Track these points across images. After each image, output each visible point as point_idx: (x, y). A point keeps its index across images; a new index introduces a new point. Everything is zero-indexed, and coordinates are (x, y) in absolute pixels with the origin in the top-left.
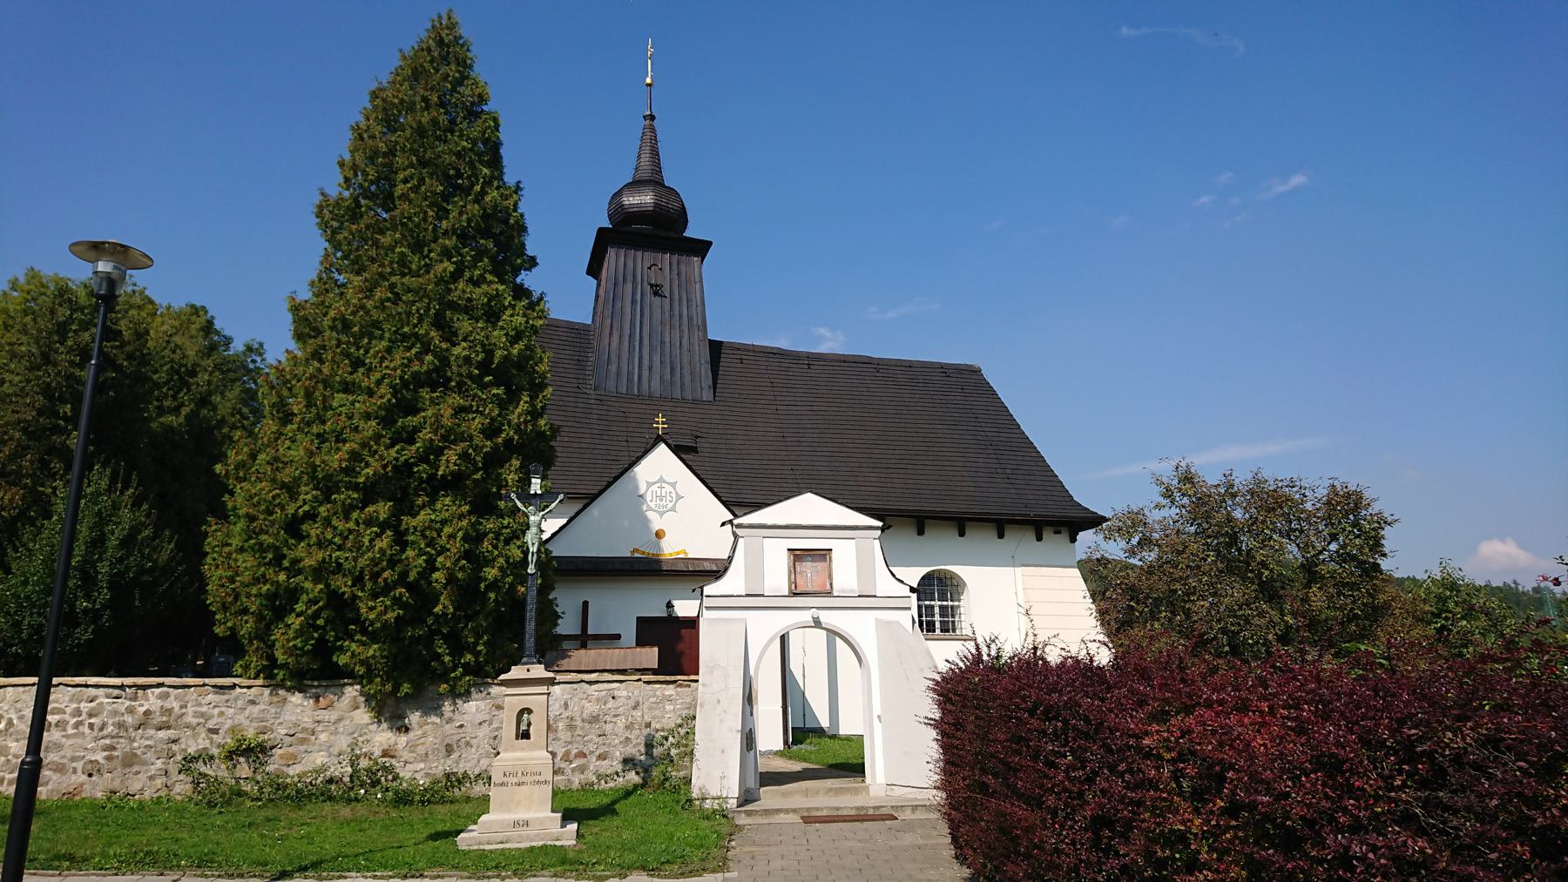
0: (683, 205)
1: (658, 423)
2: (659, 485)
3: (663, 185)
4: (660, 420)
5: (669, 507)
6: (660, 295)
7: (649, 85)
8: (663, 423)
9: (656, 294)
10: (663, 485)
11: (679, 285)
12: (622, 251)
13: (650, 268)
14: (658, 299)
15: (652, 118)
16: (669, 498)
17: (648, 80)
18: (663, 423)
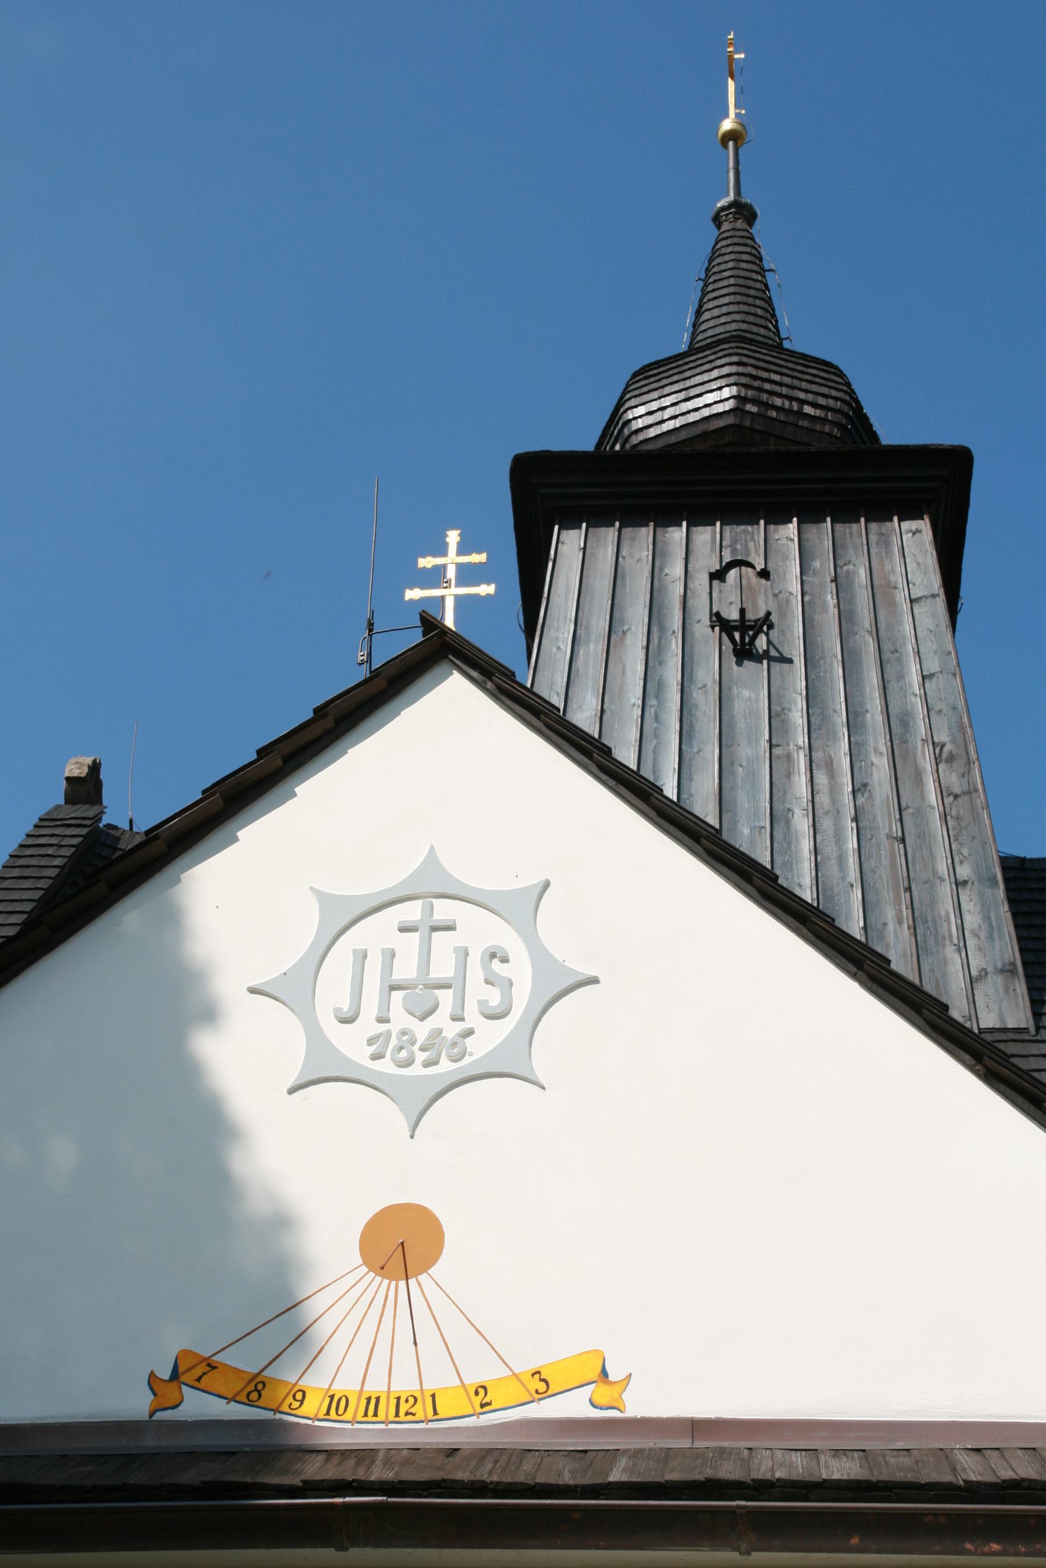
0: (852, 393)
1: (436, 577)
2: (412, 911)
3: (779, 347)
4: (452, 560)
5: (479, 1048)
6: (758, 658)
7: (732, 136)
8: (467, 575)
9: (744, 653)
10: (444, 911)
11: (846, 618)
12: (609, 534)
13: (718, 576)
14: (756, 672)
15: (743, 211)
16: (477, 990)
17: (727, 125)
18: (467, 575)
